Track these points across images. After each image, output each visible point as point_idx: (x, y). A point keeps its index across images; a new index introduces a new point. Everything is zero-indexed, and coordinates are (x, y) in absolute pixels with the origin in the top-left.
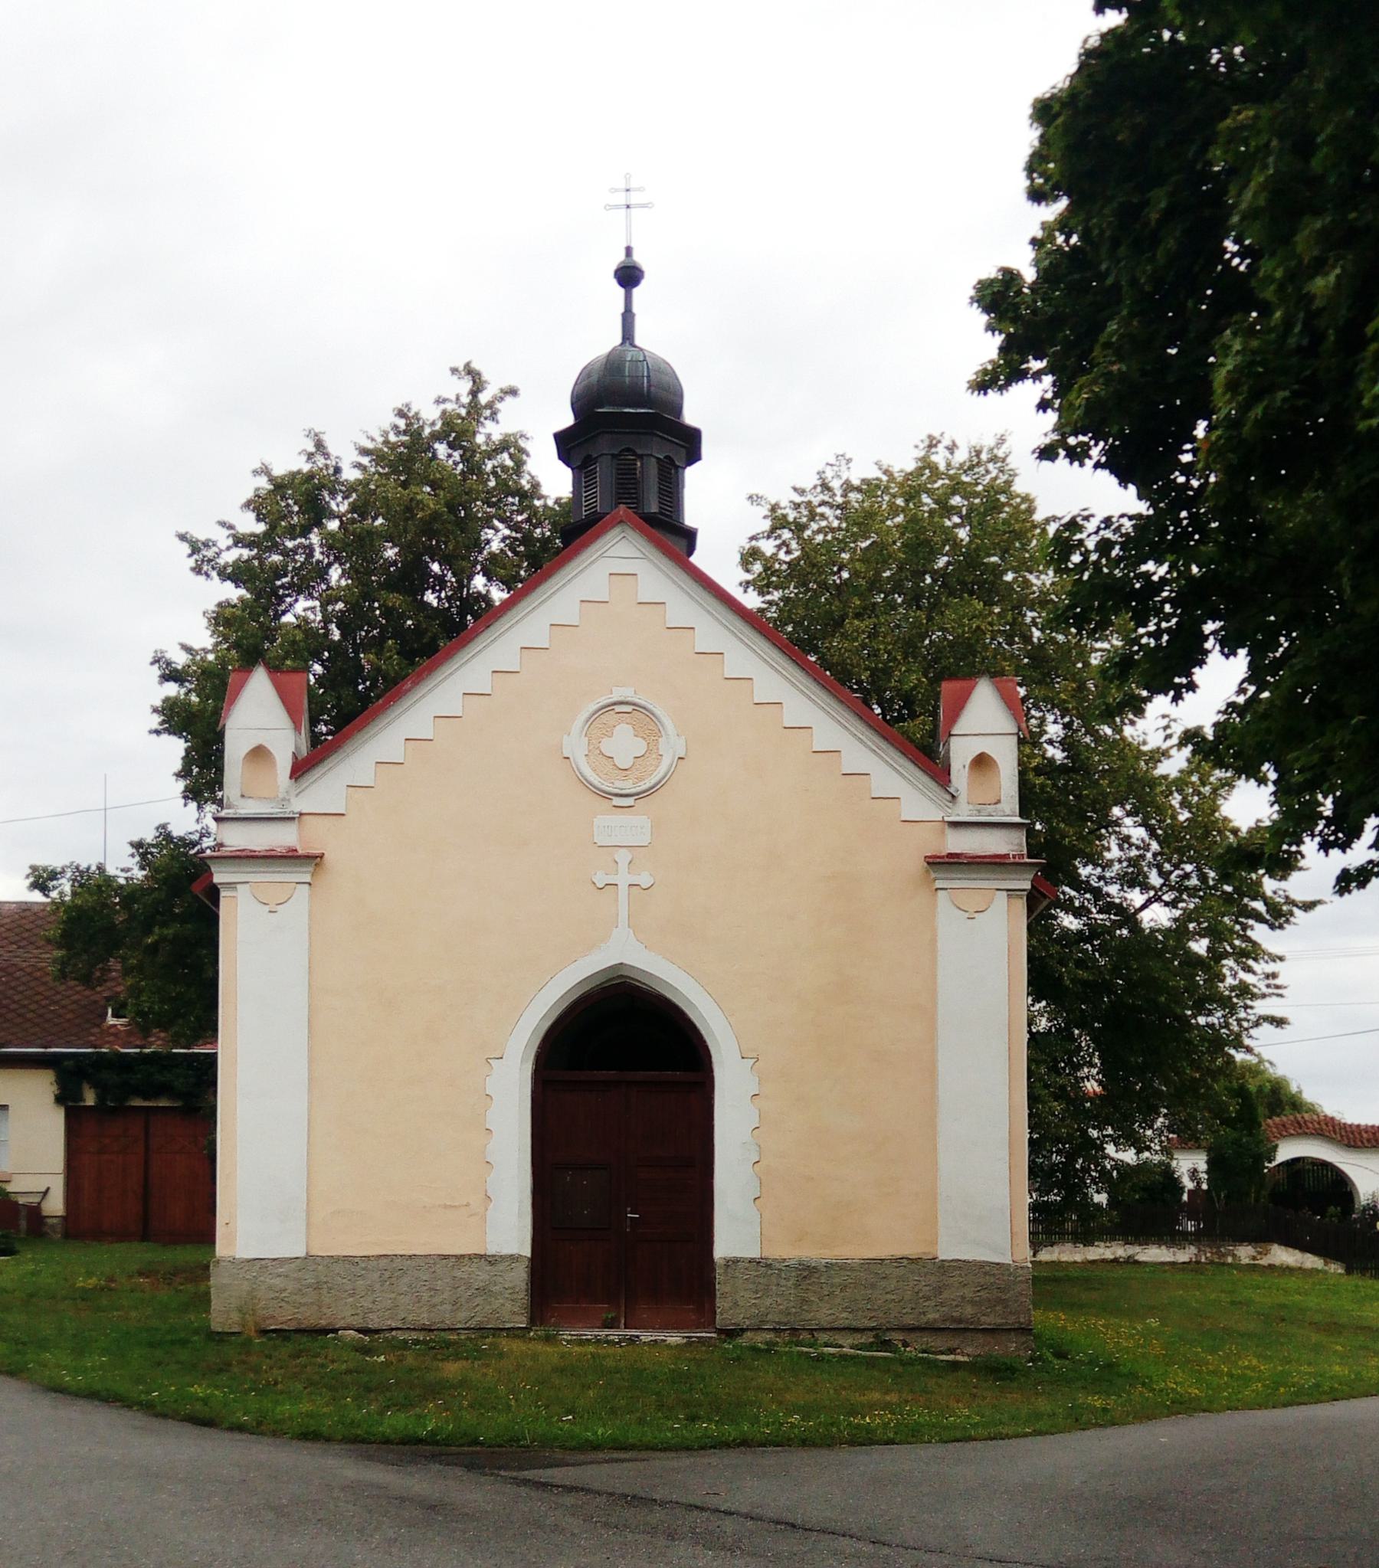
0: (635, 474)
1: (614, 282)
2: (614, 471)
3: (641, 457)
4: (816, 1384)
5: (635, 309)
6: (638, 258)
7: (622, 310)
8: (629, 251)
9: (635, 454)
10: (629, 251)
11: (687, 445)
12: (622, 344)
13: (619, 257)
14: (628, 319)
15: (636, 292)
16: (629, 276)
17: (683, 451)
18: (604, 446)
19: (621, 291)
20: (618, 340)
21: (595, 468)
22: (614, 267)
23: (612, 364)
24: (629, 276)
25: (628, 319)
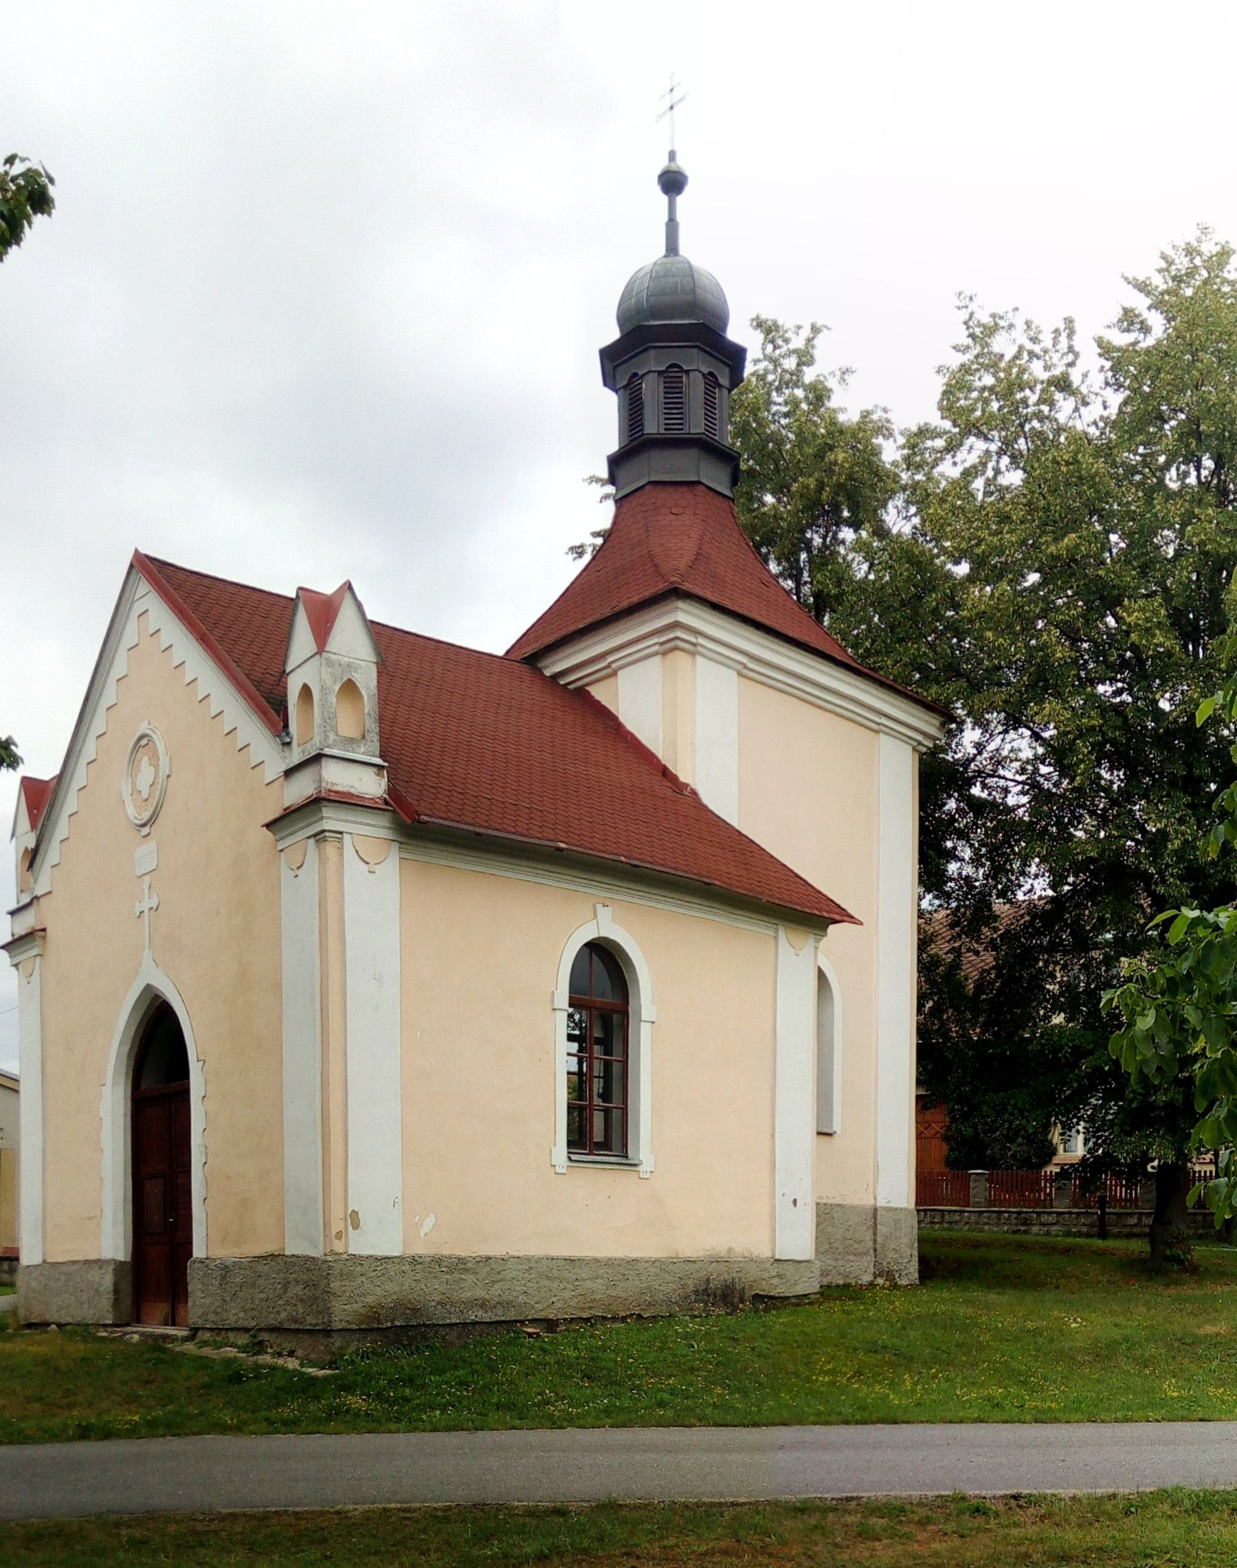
0: (665, 393)
1: (657, 189)
2: (661, 387)
3: (687, 372)
4: (504, 1360)
5: (679, 217)
6: (683, 164)
7: (666, 219)
8: (672, 156)
9: (682, 370)
10: (672, 156)
11: (730, 363)
12: (666, 256)
13: (662, 164)
14: (672, 227)
15: (680, 200)
16: (672, 183)
17: (727, 370)
18: (652, 362)
19: (665, 199)
20: (663, 252)
21: (641, 383)
22: (658, 172)
23: (658, 274)
24: (672, 183)
25: (672, 227)
